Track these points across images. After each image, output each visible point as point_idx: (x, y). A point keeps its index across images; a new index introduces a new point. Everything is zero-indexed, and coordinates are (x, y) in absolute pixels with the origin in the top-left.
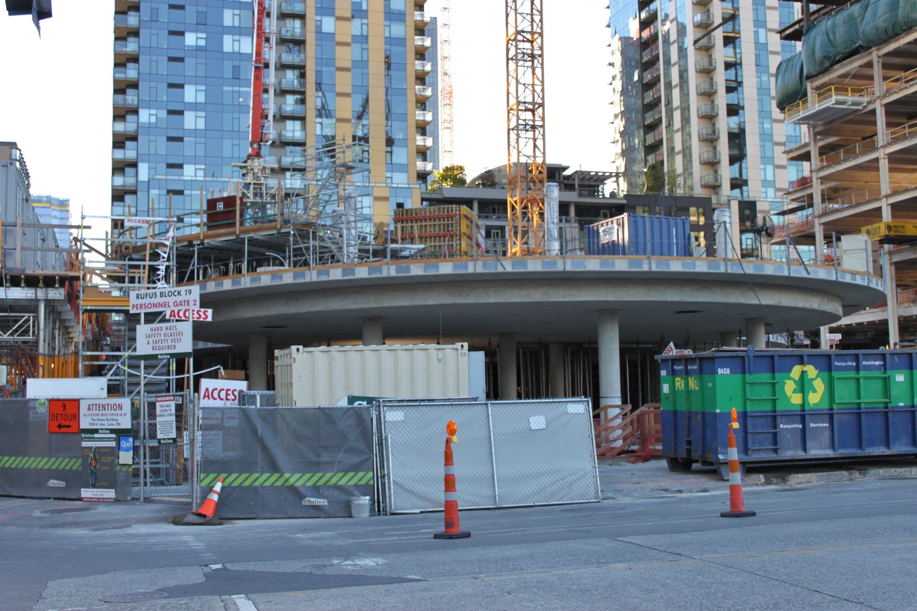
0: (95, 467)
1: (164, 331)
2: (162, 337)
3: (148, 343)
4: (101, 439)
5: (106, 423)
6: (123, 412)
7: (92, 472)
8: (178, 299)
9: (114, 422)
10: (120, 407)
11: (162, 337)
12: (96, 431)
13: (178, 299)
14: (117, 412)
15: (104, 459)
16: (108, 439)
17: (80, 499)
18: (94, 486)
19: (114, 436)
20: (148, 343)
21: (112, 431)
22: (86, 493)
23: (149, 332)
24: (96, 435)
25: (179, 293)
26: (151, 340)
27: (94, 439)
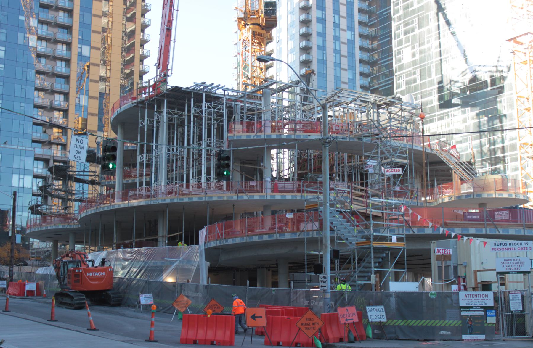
0: (471, 325)
2: (512, 264)
3: (503, 266)
4: (475, 311)
5: (478, 303)
7: (469, 327)
8: (520, 247)
10: (487, 296)
11: (512, 264)
12: (472, 307)
15: (477, 321)
16: (479, 311)
17: (463, 340)
18: (471, 333)
19: (482, 309)
20: (503, 266)
21: (481, 307)
22: (464, 337)
24: (471, 309)
26: (505, 265)
27: (469, 311)
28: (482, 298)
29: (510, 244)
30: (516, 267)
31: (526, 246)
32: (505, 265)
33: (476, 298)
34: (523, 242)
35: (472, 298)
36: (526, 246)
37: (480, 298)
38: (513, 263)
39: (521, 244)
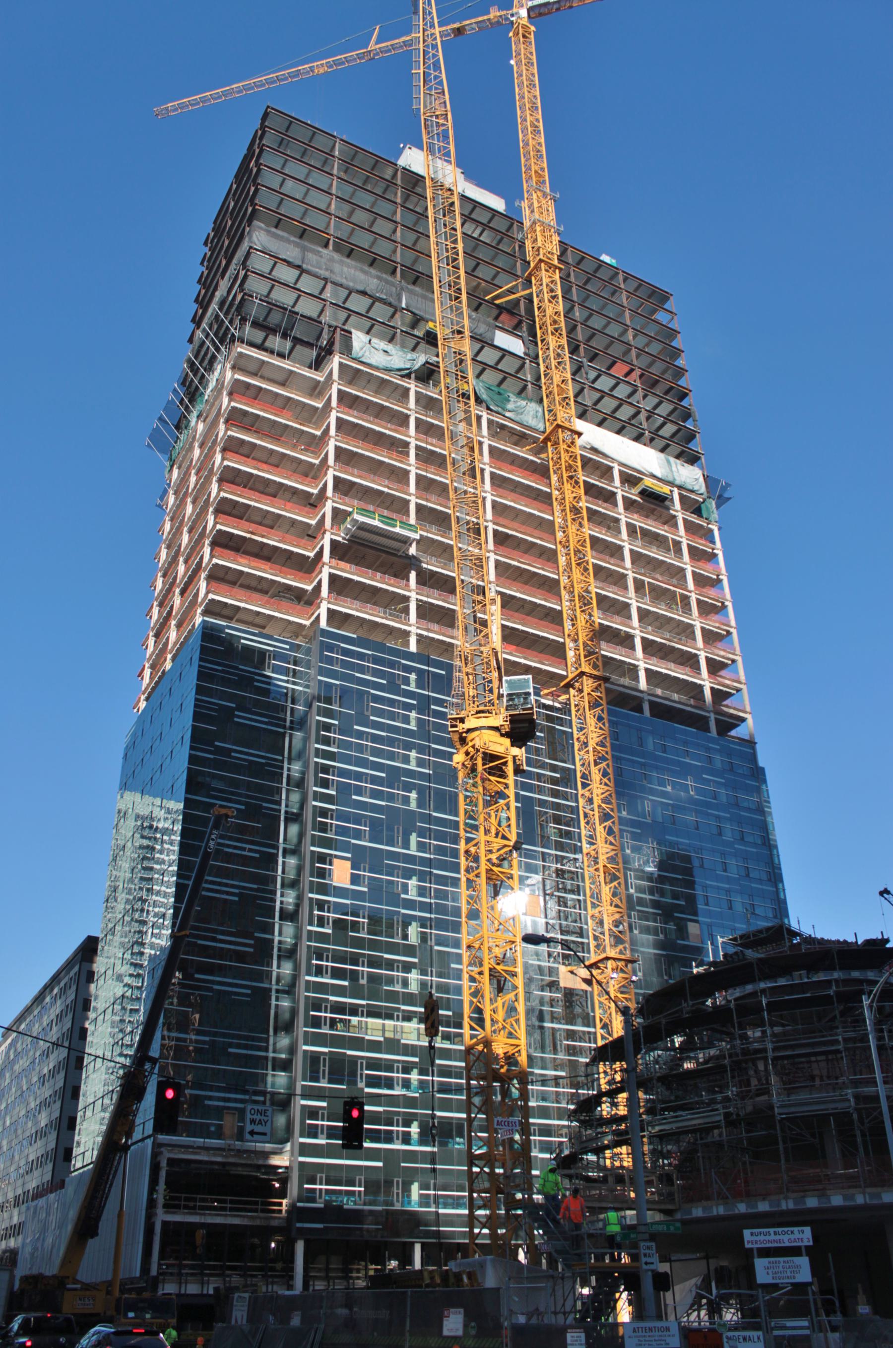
1: (782, 1264)
2: (781, 1269)
3: (768, 1274)
6: (671, 1333)
8: (792, 1237)
9: (663, 1342)
11: (781, 1269)
13: (792, 1237)
14: (665, 1333)
20: (768, 1274)
23: (767, 1265)
25: (792, 1232)
26: (770, 1271)
28: (660, 1333)
29: (775, 1233)
30: (789, 1274)
31: (801, 1236)
32: (770, 1271)
33: (651, 1334)
34: (796, 1229)
35: (644, 1334)
36: (801, 1236)
37: (657, 1333)
38: (783, 1267)
39: (792, 1232)
